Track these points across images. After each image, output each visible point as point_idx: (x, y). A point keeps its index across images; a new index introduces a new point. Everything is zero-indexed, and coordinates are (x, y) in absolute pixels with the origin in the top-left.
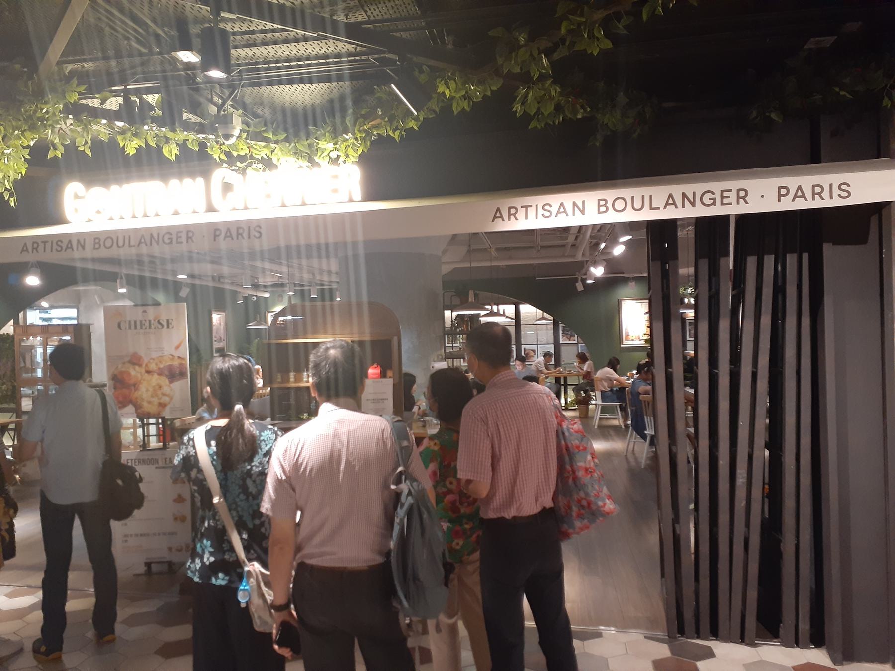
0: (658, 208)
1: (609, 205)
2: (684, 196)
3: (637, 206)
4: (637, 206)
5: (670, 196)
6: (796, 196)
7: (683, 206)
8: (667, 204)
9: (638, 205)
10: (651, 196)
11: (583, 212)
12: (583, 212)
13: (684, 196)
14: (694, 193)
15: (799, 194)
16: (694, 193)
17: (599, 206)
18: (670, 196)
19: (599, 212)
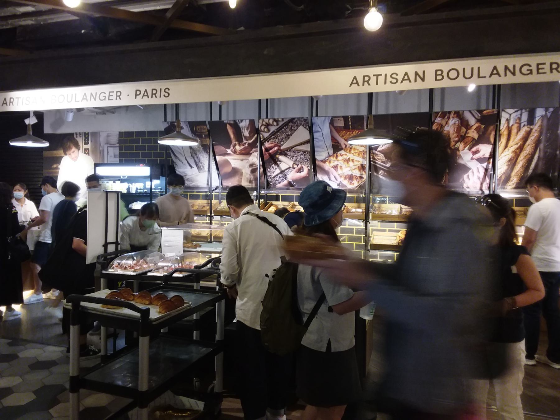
0: (485, 77)
1: (445, 74)
2: (506, 68)
3: (69, 100)
4: (468, 74)
5: (495, 68)
6: (144, 95)
7: (506, 75)
8: (492, 74)
9: (468, 74)
10: (479, 68)
11: (423, 80)
12: (423, 80)
13: (506, 68)
14: (514, 66)
15: (355, 81)
16: (514, 66)
17: (436, 75)
18: (495, 68)
19: (436, 80)
